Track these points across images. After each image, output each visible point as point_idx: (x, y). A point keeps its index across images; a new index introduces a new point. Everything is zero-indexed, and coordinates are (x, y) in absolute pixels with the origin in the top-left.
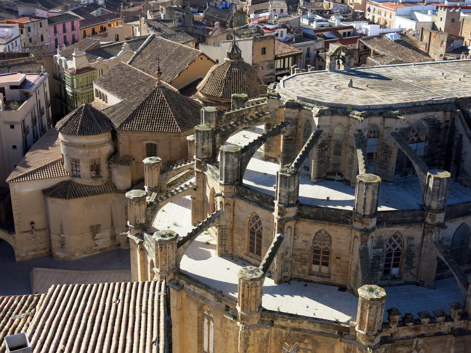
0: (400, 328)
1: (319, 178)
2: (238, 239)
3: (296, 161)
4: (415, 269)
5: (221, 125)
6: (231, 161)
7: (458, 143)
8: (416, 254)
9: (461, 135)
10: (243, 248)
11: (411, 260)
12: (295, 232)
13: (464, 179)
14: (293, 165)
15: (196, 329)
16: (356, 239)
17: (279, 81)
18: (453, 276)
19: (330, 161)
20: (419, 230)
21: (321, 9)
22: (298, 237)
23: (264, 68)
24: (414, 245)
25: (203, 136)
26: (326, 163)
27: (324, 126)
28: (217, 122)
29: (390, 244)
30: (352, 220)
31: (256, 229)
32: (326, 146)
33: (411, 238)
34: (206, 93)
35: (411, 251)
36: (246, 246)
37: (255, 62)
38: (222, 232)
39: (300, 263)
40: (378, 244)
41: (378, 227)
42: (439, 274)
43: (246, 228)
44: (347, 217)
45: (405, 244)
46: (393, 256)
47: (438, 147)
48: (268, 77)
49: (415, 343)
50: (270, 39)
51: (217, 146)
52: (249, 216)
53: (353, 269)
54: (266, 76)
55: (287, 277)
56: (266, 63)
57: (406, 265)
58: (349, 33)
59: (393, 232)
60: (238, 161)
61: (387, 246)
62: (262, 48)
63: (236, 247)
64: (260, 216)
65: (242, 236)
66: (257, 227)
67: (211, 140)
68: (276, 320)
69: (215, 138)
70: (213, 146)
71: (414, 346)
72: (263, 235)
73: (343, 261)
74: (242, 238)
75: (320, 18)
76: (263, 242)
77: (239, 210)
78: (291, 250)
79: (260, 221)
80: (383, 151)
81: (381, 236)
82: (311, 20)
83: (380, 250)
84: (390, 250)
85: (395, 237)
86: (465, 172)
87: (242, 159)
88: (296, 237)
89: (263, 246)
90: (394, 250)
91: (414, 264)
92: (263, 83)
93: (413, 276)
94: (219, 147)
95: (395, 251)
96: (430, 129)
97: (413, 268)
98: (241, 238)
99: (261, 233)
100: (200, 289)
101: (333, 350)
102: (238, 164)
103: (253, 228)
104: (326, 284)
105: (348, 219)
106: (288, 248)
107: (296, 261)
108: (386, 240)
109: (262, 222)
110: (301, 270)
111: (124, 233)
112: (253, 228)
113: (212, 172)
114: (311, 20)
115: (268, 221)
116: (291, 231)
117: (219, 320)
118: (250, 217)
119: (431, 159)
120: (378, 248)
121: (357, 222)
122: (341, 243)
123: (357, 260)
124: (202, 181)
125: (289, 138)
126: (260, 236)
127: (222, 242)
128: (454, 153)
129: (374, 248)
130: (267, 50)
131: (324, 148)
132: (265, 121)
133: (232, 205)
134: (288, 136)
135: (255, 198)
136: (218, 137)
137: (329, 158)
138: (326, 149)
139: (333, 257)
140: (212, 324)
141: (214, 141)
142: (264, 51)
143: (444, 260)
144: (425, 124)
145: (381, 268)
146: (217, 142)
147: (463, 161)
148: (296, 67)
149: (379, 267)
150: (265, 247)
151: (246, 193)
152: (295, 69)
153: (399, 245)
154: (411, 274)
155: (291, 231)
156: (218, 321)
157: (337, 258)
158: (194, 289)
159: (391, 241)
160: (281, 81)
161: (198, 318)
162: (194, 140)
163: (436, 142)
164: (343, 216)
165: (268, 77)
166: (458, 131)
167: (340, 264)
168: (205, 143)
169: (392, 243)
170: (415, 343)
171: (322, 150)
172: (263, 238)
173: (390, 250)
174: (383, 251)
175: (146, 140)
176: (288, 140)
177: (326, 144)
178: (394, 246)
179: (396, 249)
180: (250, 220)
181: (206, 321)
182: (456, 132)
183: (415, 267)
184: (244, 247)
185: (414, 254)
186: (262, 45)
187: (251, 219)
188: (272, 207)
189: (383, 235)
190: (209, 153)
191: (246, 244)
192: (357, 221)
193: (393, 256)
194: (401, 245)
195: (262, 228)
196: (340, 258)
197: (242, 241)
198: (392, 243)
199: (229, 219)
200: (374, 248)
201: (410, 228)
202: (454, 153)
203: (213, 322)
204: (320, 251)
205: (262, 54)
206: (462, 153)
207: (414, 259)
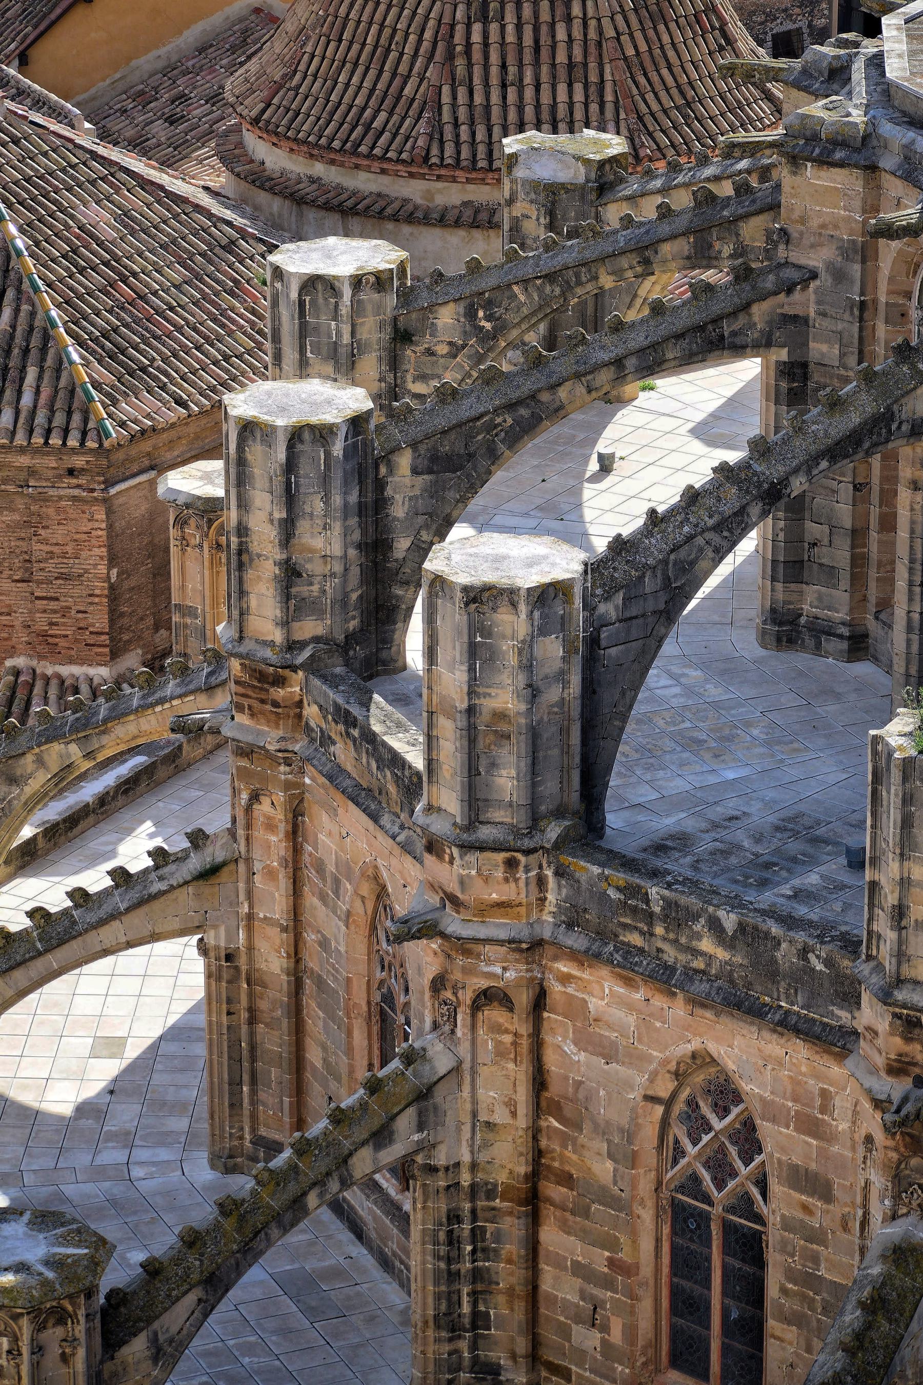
2: (579, 1270)
5: (422, 377)
6: (512, 660)
10: (616, 1335)
25: (290, 466)
28: (394, 362)
31: (720, 1184)
36: (645, 1325)
38: (454, 1217)
43: (645, 1186)
51: (402, 545)
52: (664, 1089)
63: (566, 1333)
64: (746, 1087)
65: (611, 1244)
69: (380, 485)
72: (773, 1236)
74: (611, 1263)
76: (772, 1291)
77: (584, 1041)
79: (749, 1126)
89: (772, 1325)
92: (745, 42)
94: (422, 550)
98: (599, 1259)
99: (759, 1219)
102: (566, 684)
103: (692, 1184)
109: (766, 1129)
112: (695, 1179)
118: (664, 1094)
124: (279, 815)
127: (453, 1300)
132: (762, 345)
133: (523, 999)
135: (706, 945)
146: (399, 510)
150: (791, 1333)
160: (886, 21)
172: (774, 1258)
180: (665, 1124)
184: (630, 1332)
187: (679, 1106)
190: (343, 602)
191: (646, 1306)
197: (608, 1284)
199: (500, 1116)
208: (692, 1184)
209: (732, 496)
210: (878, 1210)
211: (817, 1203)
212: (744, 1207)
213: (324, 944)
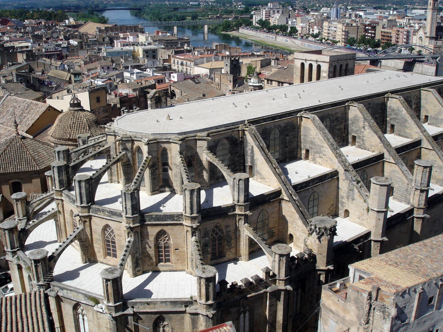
0: (230, 294)
1: (154, 191)
3: (134, 181)
4: (234, 248)
7: (251, 153)
8: (233, 237)
9: (252, 146)
11: (230, 242)
12: (141, 235)
13: (258, 178)
14: (133, 184)
15: (73, 324)
16: (188, 233)
17: (113, 121)
18: (261, 249)
19: (160, 177)
20: (233, 220)
21: (138, 64)
22: (144, 239)
23: (100, 112)
24: (229, 231)
26: (157, 179)
27: (153, 151)
29: (214, 233)
30: (183, 219)
31: (111, 237)
32: (156, 166)
33: (227, 226)
34: (57, 136)
35: (229, 235)
37: (93, 108)
39: (148, 258)
40: (205, 234)
41: (203, 222)
42: (252, 249)
44: (179, 218)
45: (224, 231)
46: (217, 242)
47: (238, 157)
48: (104, 119)
49: (241, 303)
50: (102, 90)
51: (71, 177)
53: (189, 256)
54: (103, 118)
55: (139, 271)
56: (102, 109)
57: (227, 247)
58: (162, 80)
59: (215, 224)
60: (89, 185)
61: (212, 235)
62: (97, 98)
66: (111, 236)
67: (65, 172)
68: (136, 305)
69: (68, 171)
70: (67, 177)
71: (241, 305)
72: (116, 241)
73: (181, 252)
75: (139, 71)
77: (95, 224)
78: (140, 249)
80: (199, 165)
81: (206, 228)
82: (132, 74)
83: (207, 238)
84: (214, 237)
85: (216, 227)
86: (258, 173)
87: (92, 184)
88: (143, 239)
89: (117, 250)
90: (216, 237)
91: (233, 245)
93: (234, 254)
94: (73, 177)
95: (218, 237)
96: (231, 144)
97: (232, 248)
100: (72, 292)
101: (183, 320)
104: (170, 271)
105: (180, 219)
106: (138, 248)
107: (145, 257)
108: (210, 231)
109: (114, 231)
110: (149, 263)
111: (2, 258)
113: (69, 198)
114: (132, 74)
115: (119, 230)
116: (138, 235)
117: (91, 314)
119: (234, 166)
120: (205, 237)
121: (187, 220)
122: (177, 238)
123: (191, 249)
124: (61, 206)
125: (127, 163)
126: (114, 243)
128: (249, 160)
129: (202, 238)
130: (101, 99)
131: (154, 168)
134: (125, 163)
135: (107, 213)
136: (70, 170)
137: (159, 175)
138: (157, 169)
139: (172, 249)
140: (85, 318)
141: (67, 173)
142: (98, 100)
143: (253, 238)
144: (226, 142)
145: (210, 252)
146: (70, 173)
147: (256, 165)
148: (125, 109)
149: (208, 251)
150: (119, 251)
151: (99, 211)
152: (125, 111)
153: (220, 233)
154: (231, 252)
155: (138, 235)
156: (90, 315)
157: (176, 249)
158: (67, 293)
159: (214, 231)
161: (74, 315)
162: (51, 176)
163: (236, 153)
164: (176, 217)
165: (104, 119)
166: (250, 144)
167: (179, 254)
168: (60, 176)
169: (215, 232)
170: (241, 303)
171: (153, 170)
172: (116, 243)
173: (214, 237)
174: (209, 238)
175: (11, 180)
176: (126, 165)
177: (156, 165)
178: (217, 234)
179: (218, 236)
181: (80, 316)
182: (249, 145)
183: (233, 247)
185: (232, 237)
186: (96, 95)
188: (121, 218)
189: (208, 227)
192: (187, 219)
193: (217, 242)
194: (221, 233)
195: (114, 236)
196: (178, 249)
198: (215, 232)
200: (202, 238)
201: (226, 219)
202: (249, 160)
203: (86, 316)
204: (162, 246)
205: (97, 102)
206: (255, 159)
207: (232, 241)
208: (108, 237)
209: (104, 169)
210: (127, 237)
211: (120, 238)
212: (113, 239)
213: (67, 218)
